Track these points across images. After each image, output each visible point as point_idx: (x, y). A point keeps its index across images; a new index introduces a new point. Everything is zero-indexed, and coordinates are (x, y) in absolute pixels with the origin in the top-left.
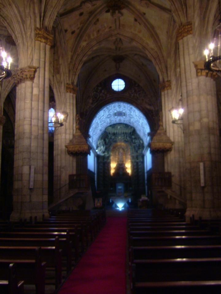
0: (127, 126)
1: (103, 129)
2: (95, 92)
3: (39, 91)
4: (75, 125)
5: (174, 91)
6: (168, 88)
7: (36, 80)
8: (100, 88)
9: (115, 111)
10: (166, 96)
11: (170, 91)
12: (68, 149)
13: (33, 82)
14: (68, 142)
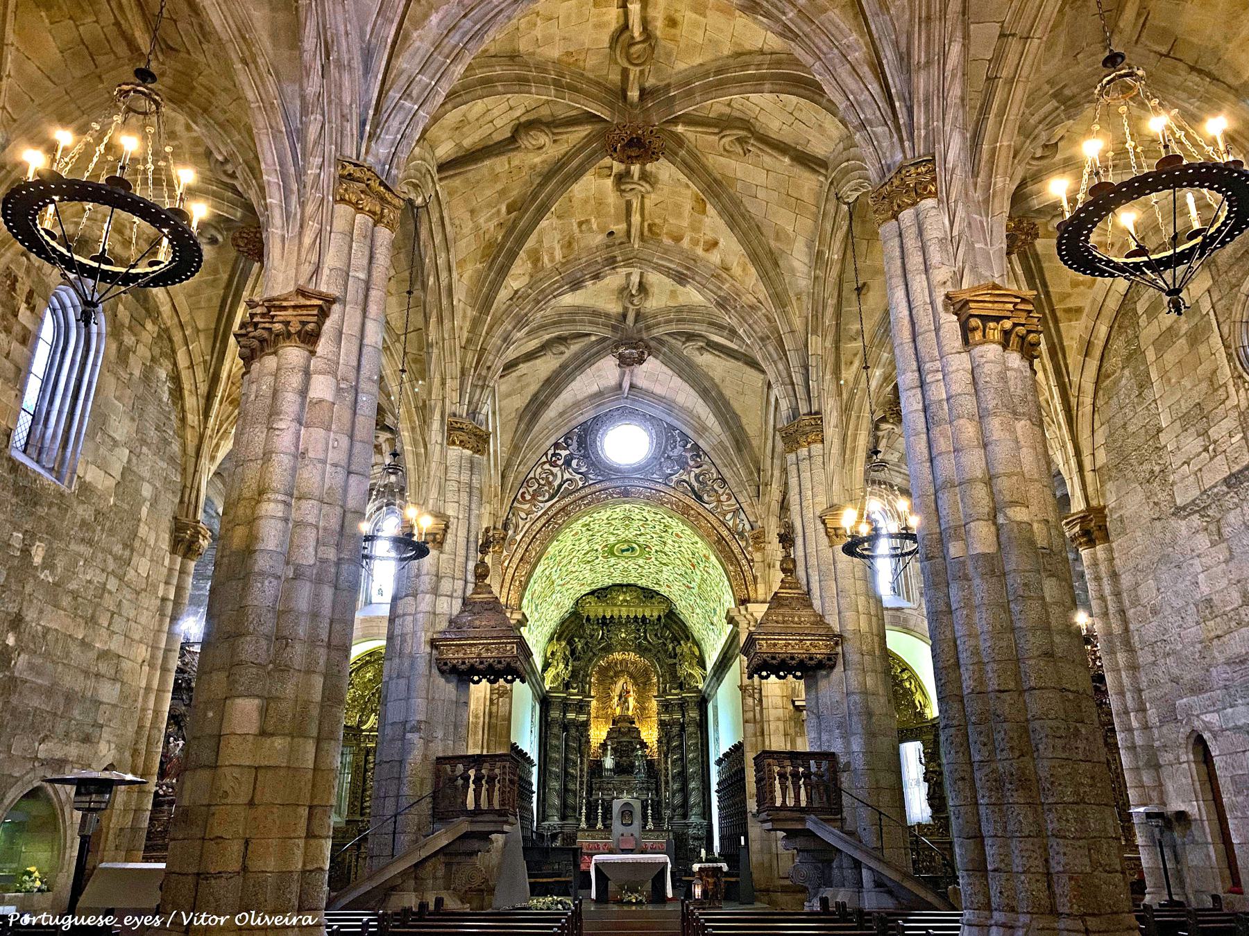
0: (648, 594)
1: (568, 604)
2: (547, 466)
3: (339, 390)
5: (835, 450)
6: (812, 437)
7: (323, 346)
8: (564, 453)
9: (612, 539)
10: (804, 465)
11: (817, 448)
13: (313, 353)
14: (443, 625)
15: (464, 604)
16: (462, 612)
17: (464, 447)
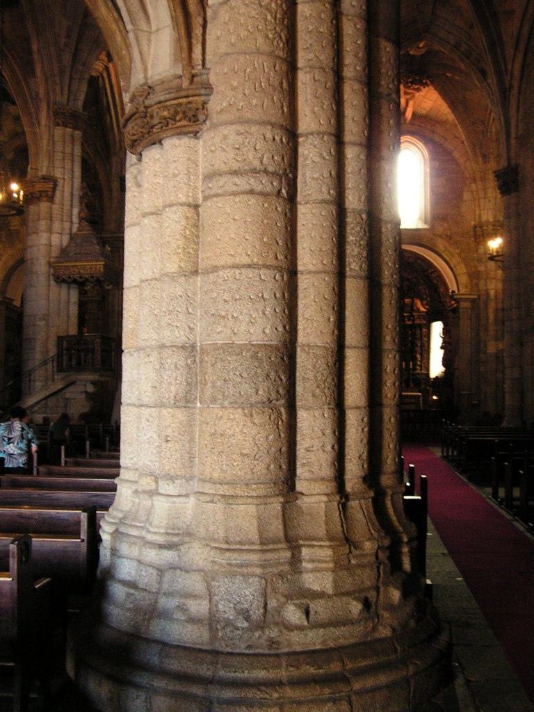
4: (76, 211)
12: (55, 271)
15: (71, 238)
16: (69, 244)
17: (66, 127)
